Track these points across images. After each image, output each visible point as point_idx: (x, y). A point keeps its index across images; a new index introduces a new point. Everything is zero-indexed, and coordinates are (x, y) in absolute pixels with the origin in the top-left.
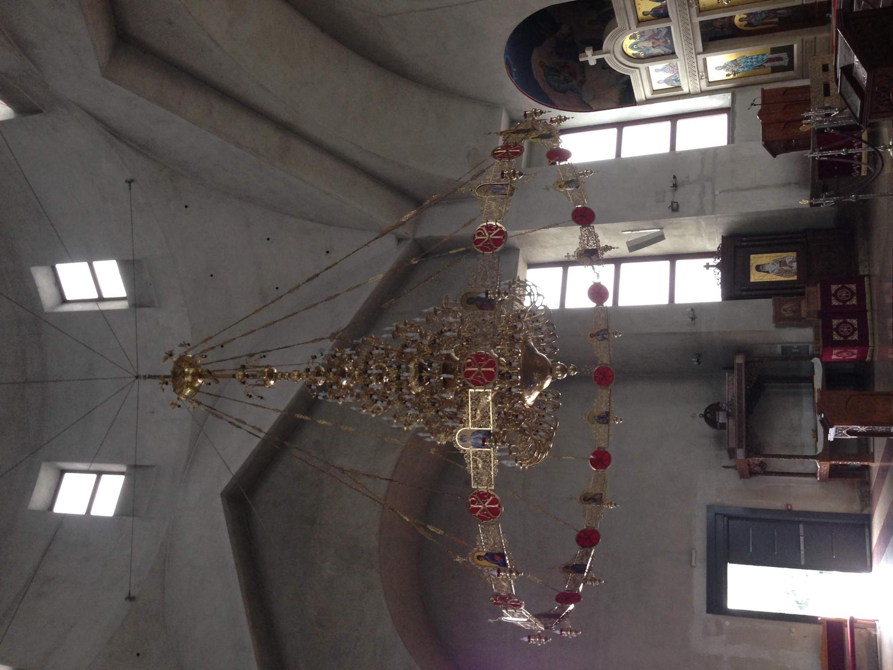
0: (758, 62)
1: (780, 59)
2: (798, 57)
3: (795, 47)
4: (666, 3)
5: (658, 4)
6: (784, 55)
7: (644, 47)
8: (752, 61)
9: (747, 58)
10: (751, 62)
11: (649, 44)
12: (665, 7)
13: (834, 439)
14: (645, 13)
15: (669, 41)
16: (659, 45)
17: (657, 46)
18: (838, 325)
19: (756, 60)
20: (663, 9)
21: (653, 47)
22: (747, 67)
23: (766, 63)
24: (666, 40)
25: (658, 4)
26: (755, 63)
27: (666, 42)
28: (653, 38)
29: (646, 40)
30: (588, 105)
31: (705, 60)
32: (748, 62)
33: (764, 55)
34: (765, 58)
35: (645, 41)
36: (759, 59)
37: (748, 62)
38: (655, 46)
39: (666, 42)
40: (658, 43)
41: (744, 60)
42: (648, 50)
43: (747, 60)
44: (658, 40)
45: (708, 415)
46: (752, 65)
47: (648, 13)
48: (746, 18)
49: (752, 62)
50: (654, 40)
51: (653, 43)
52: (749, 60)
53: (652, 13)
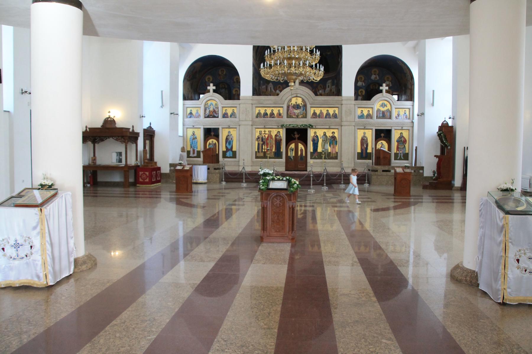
0: (194, 146)
1: (194, 153)
5: (229, 115)
6: (195, 155)
9: (197, 142)
11: (211, 109)
12: (227, 117)
13: (170, 170)
15: (211, 116)
18: (146, 174)
21: (210, 111)
23: (193, 149)
24: (212, 116)
25: (229, 115)
26: (193, 145)
27: (211, 115)
28: (213, 112)
29: (214, 109)
31: (200, 128)
32: (194, 142)
33: (197, 148)
34: (195, 149)
37: (194, 142)
39: (211, 115)
40: (211, 112)
41: (196, 141)
42: (209, 109)
44: (213, 113)
45: (110, 119)
46: (193, 144)
49: (194, 144)
51: (212, 111)
52: (195, 143)
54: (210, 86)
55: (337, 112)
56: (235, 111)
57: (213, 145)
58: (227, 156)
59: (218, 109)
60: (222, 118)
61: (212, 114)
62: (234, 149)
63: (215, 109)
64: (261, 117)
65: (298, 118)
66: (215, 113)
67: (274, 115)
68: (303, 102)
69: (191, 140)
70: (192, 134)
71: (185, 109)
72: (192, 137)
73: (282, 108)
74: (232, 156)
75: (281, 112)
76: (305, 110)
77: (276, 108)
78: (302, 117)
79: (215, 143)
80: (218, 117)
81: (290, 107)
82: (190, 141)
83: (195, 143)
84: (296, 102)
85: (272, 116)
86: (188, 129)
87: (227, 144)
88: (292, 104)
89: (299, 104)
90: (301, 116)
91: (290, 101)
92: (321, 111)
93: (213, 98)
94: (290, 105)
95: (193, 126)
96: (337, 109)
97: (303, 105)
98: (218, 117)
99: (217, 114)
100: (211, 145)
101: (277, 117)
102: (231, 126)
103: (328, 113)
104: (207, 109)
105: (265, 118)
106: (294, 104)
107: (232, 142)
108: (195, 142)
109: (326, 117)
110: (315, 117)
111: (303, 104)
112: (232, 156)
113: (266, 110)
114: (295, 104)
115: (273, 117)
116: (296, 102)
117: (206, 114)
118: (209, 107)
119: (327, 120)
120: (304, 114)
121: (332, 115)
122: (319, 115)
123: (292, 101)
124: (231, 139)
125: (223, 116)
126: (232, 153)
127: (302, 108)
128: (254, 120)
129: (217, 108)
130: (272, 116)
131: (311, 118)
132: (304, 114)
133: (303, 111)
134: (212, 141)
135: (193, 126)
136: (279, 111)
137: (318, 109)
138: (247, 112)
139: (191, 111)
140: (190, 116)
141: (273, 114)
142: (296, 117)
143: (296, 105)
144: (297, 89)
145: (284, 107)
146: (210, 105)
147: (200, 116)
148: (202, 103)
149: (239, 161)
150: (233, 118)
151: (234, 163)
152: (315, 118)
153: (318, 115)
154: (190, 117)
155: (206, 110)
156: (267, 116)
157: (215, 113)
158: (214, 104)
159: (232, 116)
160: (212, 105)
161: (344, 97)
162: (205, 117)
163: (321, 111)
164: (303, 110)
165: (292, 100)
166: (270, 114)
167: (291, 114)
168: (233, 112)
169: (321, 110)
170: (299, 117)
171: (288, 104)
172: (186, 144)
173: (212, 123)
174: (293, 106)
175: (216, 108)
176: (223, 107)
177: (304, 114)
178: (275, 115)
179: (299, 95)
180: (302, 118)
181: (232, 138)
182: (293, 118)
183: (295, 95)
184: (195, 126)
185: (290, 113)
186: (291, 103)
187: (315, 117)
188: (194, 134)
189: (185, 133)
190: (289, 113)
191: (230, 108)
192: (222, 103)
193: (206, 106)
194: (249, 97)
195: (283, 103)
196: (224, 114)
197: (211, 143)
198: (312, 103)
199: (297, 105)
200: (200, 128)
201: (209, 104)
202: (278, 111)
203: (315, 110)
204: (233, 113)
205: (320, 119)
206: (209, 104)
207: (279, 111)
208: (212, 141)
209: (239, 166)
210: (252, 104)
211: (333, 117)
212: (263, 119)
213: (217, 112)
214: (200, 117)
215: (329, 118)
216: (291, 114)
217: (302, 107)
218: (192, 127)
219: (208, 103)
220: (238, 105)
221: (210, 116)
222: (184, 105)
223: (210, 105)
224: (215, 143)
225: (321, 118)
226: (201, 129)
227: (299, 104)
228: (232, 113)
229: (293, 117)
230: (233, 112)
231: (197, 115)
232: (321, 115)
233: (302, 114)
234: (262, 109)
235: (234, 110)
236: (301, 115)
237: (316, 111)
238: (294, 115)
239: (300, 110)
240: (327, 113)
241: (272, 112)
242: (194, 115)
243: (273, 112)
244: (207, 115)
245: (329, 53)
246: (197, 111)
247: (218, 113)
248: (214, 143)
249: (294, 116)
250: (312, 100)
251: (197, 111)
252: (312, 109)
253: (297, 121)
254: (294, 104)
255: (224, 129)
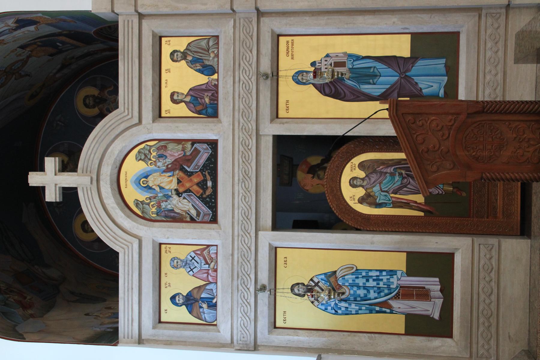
0: (379, 290)
2: (463, 273)
3: (458, 261)
4: (217, 80)
5: (201, 79)
7: (161, 188)
8: (368, 284)
9: (357, 272)
10: (365, 288)
14: (175, 97)
15: (209, 184)
16: (188, 191)
17: (185, 192)
19: (374, 284)
20: (210, 94)
21: (178, 194)
22: (355, 300)
23: (397, 297)
24: (205, 181)
25: (201, 79)
26: (372, 294)
27: (202, 185)
28: (182, 169)
29: (167, 170)
30: (22, 335)
31: (274, 251)
32: (359, 287)
33: (392, 273)
34: (395, 282)
35: (165, 171)
36: (381, 285)
37: (359, 287)
38: (181, 190)
40: (188, 185)
42: (167, 197)
43: (357, 281)
46: (365, 298)
47: (180, 98)
48: (363, 179)
50: (181, 174)
51: (179, 182)
52: (361, 282)
53: (188, 99)
54: (43, 188)
56: (181, 44)
57: (374, 177)
58: (442, 93)
59: (171, 146)
60: (220, 122)
61: (196, 180)
62: (406, 53)
63: (169, 160)
66: (189, 160)
69: (343, 304)
70: (306, 301)
71: (164, 332)
72: (324, 296)
74: (439, 64)
79: (362, 166)
80: (213, 144)
82: (347, 313)
83: (361, 282)
86: (280, 323)
87: (366, 88)
93: (107, 171)
95: (263, 288)
98: (213, 144)
99: (196, 152)
100: (376, 189)
102: (266, 66)
104: (169, 207)
107: (358, 58)
108: (352, 285)
112: (439, 64)
117: (193, 212)
118: (160, 195)
124: (338, 64)
125: (209, 116)
126: (424, 58)
129: (165, 147)
134: (353, 182)
135: (263, 288)
139: (178, 300)
140: (205, 306)
146: (149, 188)
147: (208, 246)
148: (135, 231)
149: (477, 10)
150: (217, 56)
151: (489, 45)
154: (213, 306)
155: (172, 211)
157: (189, 160)
158: (142, 166)
159: (210, 61)
160: (146, 177)
162: (214, 220)
168: (184, 55)
172: (364, 338)
173: (246, 174)
175: (161, 156)
176: (158, 115)
181: (332, 61)
184: (264, 278)
188: (309, 290)
189: (303, 339)
191: (164, 76)
192: (136, 120)
193: (152, 210)
196: (199, 112)
197: (360, 192)
200: (274, 251)
201: (142, 196)
204: (190, 58)
206: (142, 196)
208: (353, 182)
209: (508, 6)
213: (183, 149)
214: (213, 250)
218: (263, 297)
219: (137, 203)
220: (145, 23)
221: (209, 192)
222: (140, 341)
223: (149, 188)
224: (362, 166)
226: (276, 244)
228: (192, 63)
230: (184, 55)
231: (200, 265)
235: (172, 54)
242: (203, 283)
244: (204, 209)
246: (176, 263)
247: (194, 142)
248: (362, 174)
251: (175, 267)
255: (282, 113)
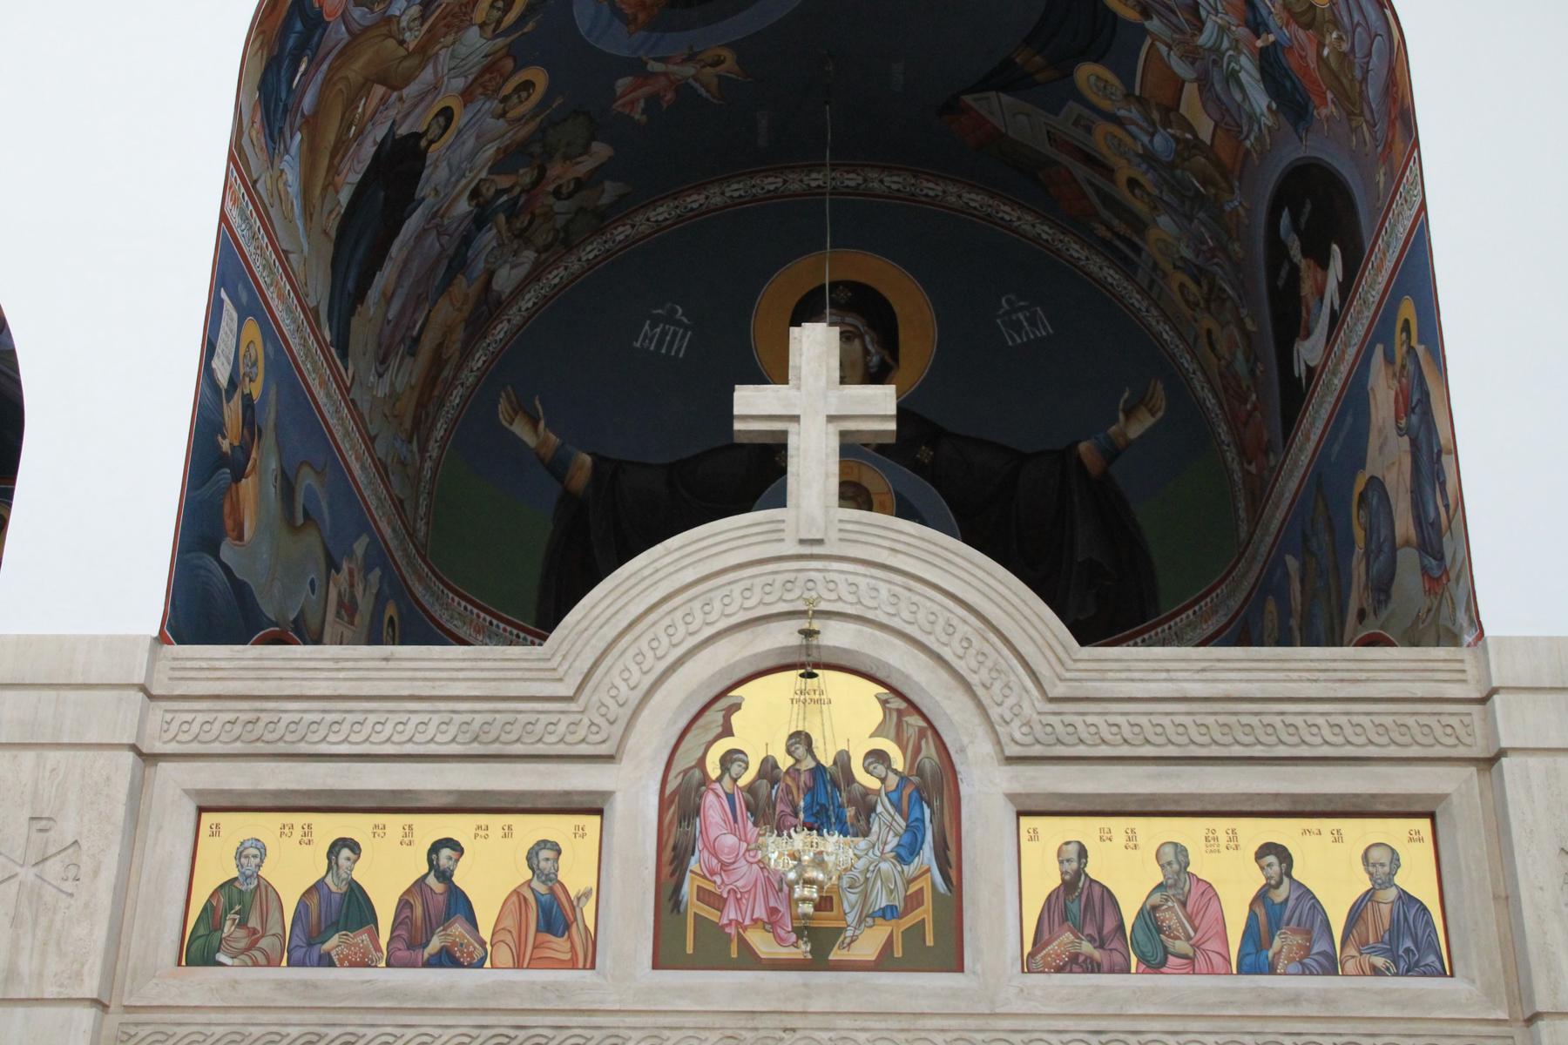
55: (1417, 878)
64: (252, 953)
65: (818, 962)
67: (458, 929)
68: (899, 740)
73: (597, 819)
75: (576, 874)
76: (927, 852)
77: (496, 822)
78: (889, 944)
81: (713, 809)
84: (800, 740)
85: (435, 944)
88: (728, 759)
89: (843, 760)
90: (868, 945)
91: (715, 716)
92: (1175, 859)
94: (713, 770)
96: (1414, 837)
97: (903, 779)
101: (504, 955)
103: (1280, 895)
105: (326, 961)
106: (769, 769)
109: (1256, 959)
110: (1087, 947)
111: (899, 762)
113: (354, 846)
114: (785, 762)
115: (447, 959)
116: (800, 740)
119: (1295, 999)
120: (914, 901)
121: (1356, 915)
122: (1149, 915)
123: (736, 719)
127: (887, 826)
128: (151, 993)
130: (435, 944)
131: (1029, 965)
132: (925, 912)
133: (911, 870)
136: (542, 855)
137: (1131, 836)
138: (53, 868)
141: (459, 905)
142: (803, 950)
143: (793, 771)
144: (812, 549)
145: (618, 809)
152: (1093, 967)
153: (1129, 919)
156: (363, 938)
161: (1499, 640)
163: (1175, 859)
164: (907, 851)
165: (737, 707)
166: (404, 904)
167: (718, 902)
169: (1180, 850)
170: (835, 955)
171: (685, 760)
174: (751, 789)
177: (914, 901)
178: (486, 932)
179: (835, 636)
180: (884, 962)
182: (750, 960)
183: (784, 636)
185: (704, 895)
186: (724, 745)
187: (1087, 947)
190: (688, 889)
194: (116, 645)
195: (603, 750)
198: (1037, 750)
199: (819, 766)
202: (532, 856)
203: (1083, 853)
205: (1170, 982)
207: (542, 855)
210: (149, 759)
211: (1363, 945)
212: (282, 985)
215: (1306, 971)
216: (731, 913)
217: (883, 808)
225: (1190, 964)
227: (843, 760)
229: (743, 943)
232: (1172, 917)
233: (888, 913)
234: (285, 830)
236: (870, 916)
237: (1093, 870)
238: (771, 922)
239: (862, 843)
240: (1262, 897)
241: (445, 876)
243: (457, 879)
245: (1136, 430)
249: (762, 943)
250: (1032, 704)
252: (1054, 832)
253: (817, 1005)
254: (769, 769)
